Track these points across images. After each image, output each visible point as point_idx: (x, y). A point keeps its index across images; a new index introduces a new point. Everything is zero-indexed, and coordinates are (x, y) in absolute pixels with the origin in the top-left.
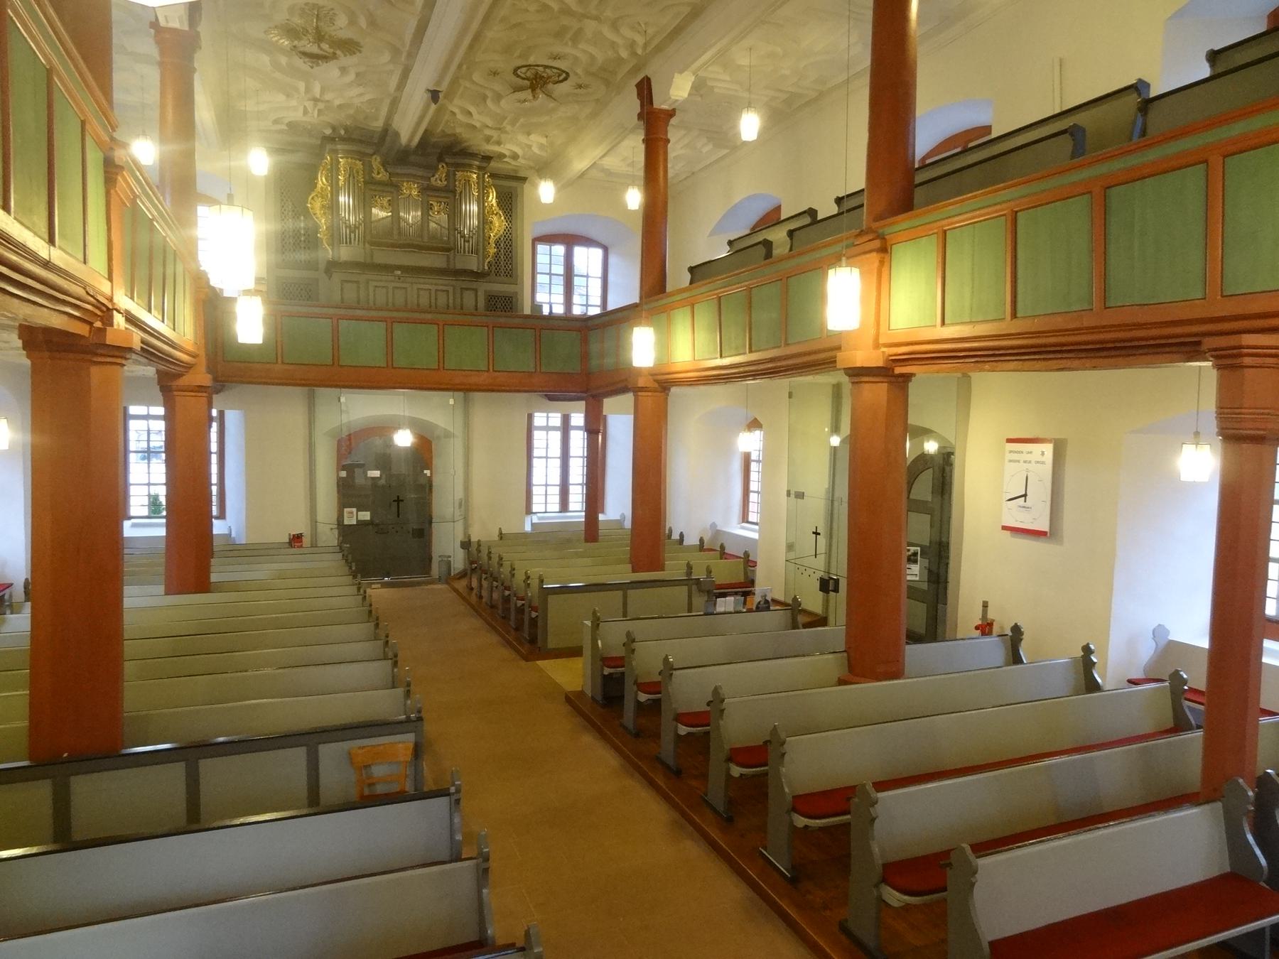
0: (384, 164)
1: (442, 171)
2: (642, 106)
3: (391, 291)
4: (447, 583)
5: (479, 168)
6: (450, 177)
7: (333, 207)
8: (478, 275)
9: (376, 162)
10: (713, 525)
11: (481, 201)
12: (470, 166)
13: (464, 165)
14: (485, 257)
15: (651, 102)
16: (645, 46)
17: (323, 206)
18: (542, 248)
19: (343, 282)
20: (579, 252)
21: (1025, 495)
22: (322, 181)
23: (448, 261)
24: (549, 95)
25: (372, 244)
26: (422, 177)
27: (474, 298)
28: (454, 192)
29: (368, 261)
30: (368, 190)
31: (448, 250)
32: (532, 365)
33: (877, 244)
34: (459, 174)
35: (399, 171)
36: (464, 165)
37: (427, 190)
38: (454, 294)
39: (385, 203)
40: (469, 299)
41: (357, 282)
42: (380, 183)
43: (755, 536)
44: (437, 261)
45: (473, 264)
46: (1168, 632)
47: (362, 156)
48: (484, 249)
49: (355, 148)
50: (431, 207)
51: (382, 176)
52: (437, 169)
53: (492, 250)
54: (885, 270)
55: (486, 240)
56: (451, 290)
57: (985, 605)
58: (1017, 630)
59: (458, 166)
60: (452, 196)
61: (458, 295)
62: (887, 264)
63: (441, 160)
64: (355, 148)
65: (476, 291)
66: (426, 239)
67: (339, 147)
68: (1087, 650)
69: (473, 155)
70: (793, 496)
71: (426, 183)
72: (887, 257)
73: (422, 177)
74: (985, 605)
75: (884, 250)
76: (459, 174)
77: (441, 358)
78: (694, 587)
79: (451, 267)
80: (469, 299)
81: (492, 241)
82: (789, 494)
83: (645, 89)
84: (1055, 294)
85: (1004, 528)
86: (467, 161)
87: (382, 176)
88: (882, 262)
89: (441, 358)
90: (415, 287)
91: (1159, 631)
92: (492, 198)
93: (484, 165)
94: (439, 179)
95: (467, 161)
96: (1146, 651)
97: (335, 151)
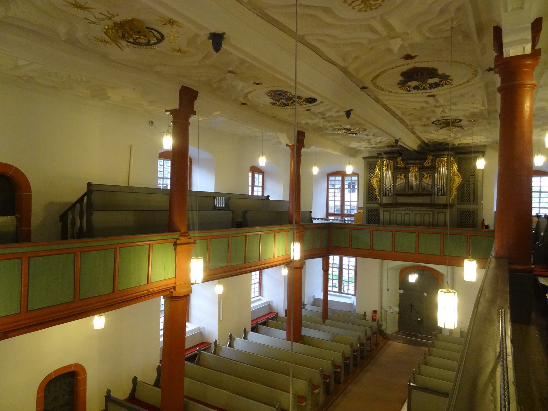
0: (402, 160)
1: (430, 158)
5: (448, 155)
6: (433, 161)
7: (381, 181)
9: (399, 160)
12: (444, 155)
13: (441, 155)
14: (450, 197)
16: (483, 105)
19: (384, 211)
22: (377, 170)
23: (431, 201)
25: (396, 195)
30: (396, 170)
31: (431, 195)
34: (437, 159)
35: (409, 162)
36: (441, 155)
37: (422, 170)
38: (433, 215)
39: (402, 176)
40: (441, 217)
41: (390, 211)
45: (442, 200)
49: (390, 156)
51: (401, 165)
52: (426, 159)
53: (454, 192)
55: (451, 189)
56: (431, 213)
60: (433, 169)
63: (427, 155)
64: (390, 156)
65: (445, 213)
71: (421, 165)
76: (437, 159)
80: (441, 217)
86: (442, 153)
90: (414, 212)
92: (455, 166)
97: (383, 158)
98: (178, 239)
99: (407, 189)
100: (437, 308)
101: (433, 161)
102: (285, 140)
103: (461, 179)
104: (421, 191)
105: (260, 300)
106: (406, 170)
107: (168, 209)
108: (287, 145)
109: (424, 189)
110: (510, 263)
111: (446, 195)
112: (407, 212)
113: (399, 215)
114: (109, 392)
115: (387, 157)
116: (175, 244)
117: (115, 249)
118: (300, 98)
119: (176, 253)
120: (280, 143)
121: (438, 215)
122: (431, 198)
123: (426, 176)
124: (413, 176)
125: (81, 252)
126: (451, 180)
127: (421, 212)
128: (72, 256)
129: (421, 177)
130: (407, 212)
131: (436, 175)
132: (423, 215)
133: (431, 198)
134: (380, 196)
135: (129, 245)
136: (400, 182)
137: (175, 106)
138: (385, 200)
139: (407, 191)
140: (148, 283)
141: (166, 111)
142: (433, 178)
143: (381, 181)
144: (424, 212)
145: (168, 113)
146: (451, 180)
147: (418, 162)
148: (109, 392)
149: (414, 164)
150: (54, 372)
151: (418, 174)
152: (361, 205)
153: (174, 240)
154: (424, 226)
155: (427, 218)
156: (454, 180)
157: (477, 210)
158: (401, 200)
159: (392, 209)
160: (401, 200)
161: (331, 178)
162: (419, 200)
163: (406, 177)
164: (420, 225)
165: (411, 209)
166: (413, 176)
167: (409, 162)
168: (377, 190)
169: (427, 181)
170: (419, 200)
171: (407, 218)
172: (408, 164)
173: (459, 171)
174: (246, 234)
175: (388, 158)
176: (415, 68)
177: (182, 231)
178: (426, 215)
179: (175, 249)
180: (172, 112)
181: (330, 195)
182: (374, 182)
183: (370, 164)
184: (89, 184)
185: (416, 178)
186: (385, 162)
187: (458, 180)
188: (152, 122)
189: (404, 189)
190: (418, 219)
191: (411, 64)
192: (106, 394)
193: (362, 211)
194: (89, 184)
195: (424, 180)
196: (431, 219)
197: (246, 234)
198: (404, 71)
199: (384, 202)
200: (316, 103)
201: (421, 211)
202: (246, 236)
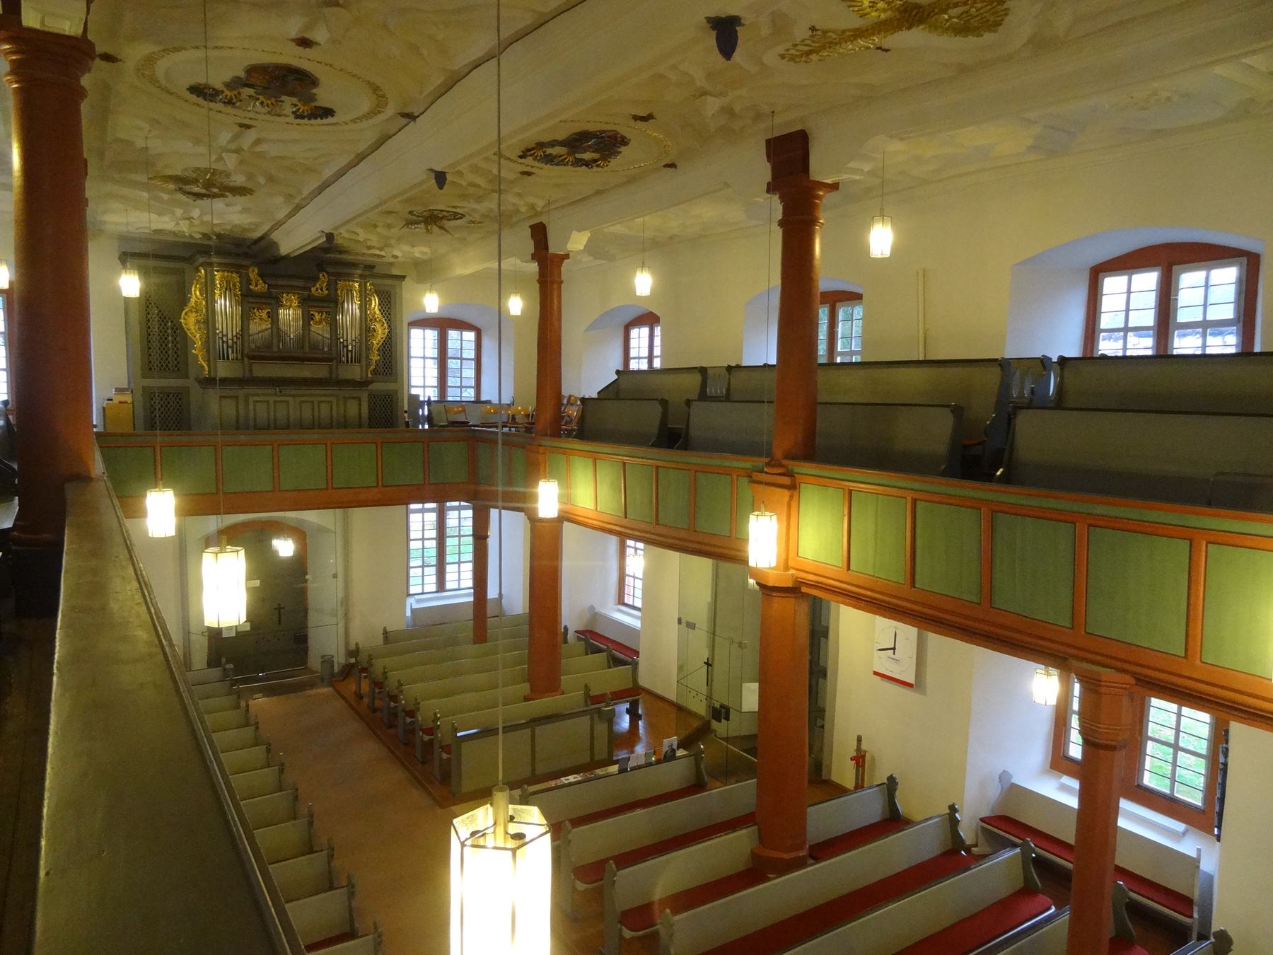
1: (324, 278)
2: (536, 247)
3: (272, 405)
4: (331, 684)
5: (361, 276)
7: (208, 320)
8: (363, 384)
9: (253, 273)
10: (592, 608)
11: (364, 307)
12: (352, 275)
14: (368, 365)
15: (547, 248)
17: (198, 322)
18: (416, 333)
19: (221, 397)
20: (453, 334)
21: (894, 649)
22: (196, 294)
23: (331, 372)
24: (442, 228)
27: (357, 408)
28: (336, 302)
29: (247, 374)
31: (331, 360)
32: (421, 476)
33: (786, 480)
34: (341, 284)
37: (307, 303)
39: (264, 314)
41: (236, 397)
43: (636, 624)
44: (320, 371)
46: (1011, 777)
47: (238, 268)
48: (367, 357)
50: (311, 317)
51: (260, 287)
52: (316, 279)
53: (375, 357)
54: (794, 504)
55: (369, 348)
57: (859, 740)
58: (891, 779)
59: (339, 276)
60: (332, 304)
61: (341, 402)
62: (795, 498)
66: (307, 349)
67: (215, 260)
68: (953, 809)
69: (354, 265)
70: (684, 625)
71: (306, 293)
72: (796, 493)
74: (859, 740)
75: (793, 487)
76: (341, 284)
78: (596, 716)
81: (376, 347)
82: (680, 621)
83: (539, 233)
84: (943, 577)
85: (876, 673)
86: (345, 271)
88: (791, 497)
90: (298, 399)
91: (1004, 776)
93: (367, 273)
94: (319, 288)
95: (345, 271)
96: (994, 792)
101: (332, 286)
104: (305, 352)
106: (271, 301)
109: (314, 347)
112: (278, 399)
113: (261, 405)
115: (219, 264)
123: (317, 317)
124: (290, 315)
129: (308, 318)
130: (278, 399)
131: (339, 317)
134: (209, 361)
136: (259, 326)
138: (223, 370)
142: (334, 325)
147: (301, 283)
149: (290, 289)
151: (299, 312)
154: (320, 428)
155: (325, 411)
157: (396, 392)
158: (261, 370)
159: (241, 393)
160: (261, 370)
162: (305, 372)
163: (273, 316)
164: (268, 427)
166: (290, 315)
167: (280, 282)
169: (320, 330)
170: (305, 372)
172: (277, 287)
175: (224, 267)
178: (325, 405)
182: (190, 322)
185: (295, 320)
186: (218, 275)
187: (381, 332)
189: (269, 346)
190: (307, 414)
193: (128, 398)
195: (314, 328)
201: (310, 395)
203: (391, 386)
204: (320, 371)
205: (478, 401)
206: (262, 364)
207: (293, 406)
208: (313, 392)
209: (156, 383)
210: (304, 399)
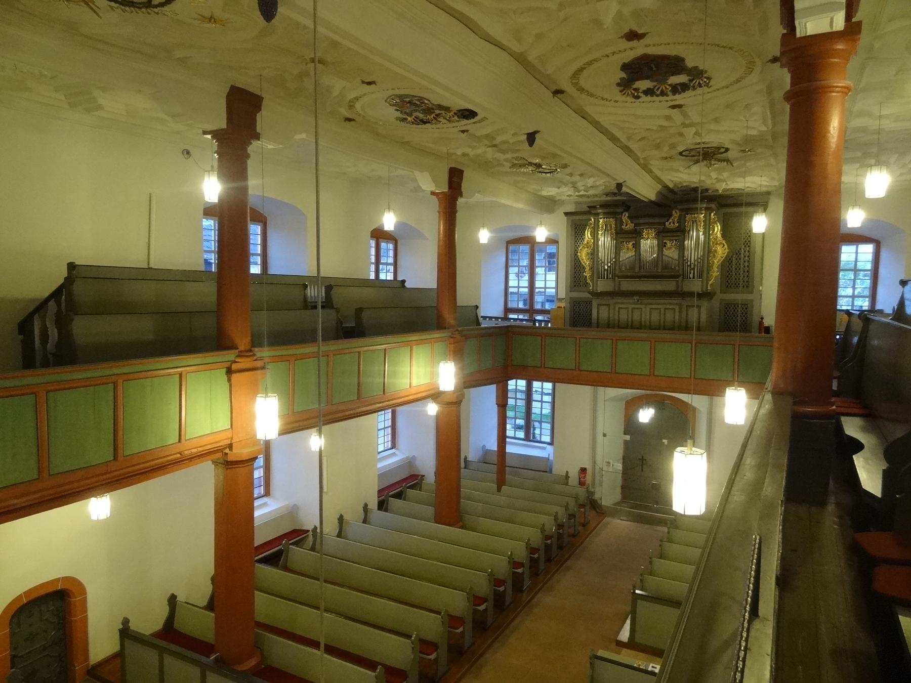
1: (676, 214)
5: (706, 209)
6: (681, 220)
7: (594, 254)
9: (625, 217)
14: (708, 280)
16: (765, 123)
22: (588, 235)
26: (660, 224)
27: (699, 313)
30: (620, 235)
34: (688, 217)
36: (693, 209)
37: (663, 234)
38: (680, 312)
39: (630, 245)
41: (608, 305)
42: (627, 232)
44: (670, 286)
45: (696, 286)
47: (613, 214)
49: (612, 210)
51: (630, 226)
52: (671, 216)
53: (715, 273)
55: (710, 267)
56: (677, 308)
60: (681, 233)
63: (671, 209)
67: (600, 211)
71: (662, 227)
73: (660, 224)
77: (652, 366)
79: (680, 290)
80: (693, 315)
87: (630, 226)
89: (652, 366)
90: (649, 307)
92: (718, 228)
97: (598, 214)
98: (235, 362)
99: (637, 270)
100: (671, 480)
101: (681, 220)
102: (429, 183)
103: (727, 250)
104: (662, 271)
105: (394, 454)
106: (636, 235)
107: (214, 308)
108: (433, 193)
109: (666, 267)
110: (795, 403)
111: (700, 276)
113: (624, 311)
114: (126, 622)
115: (604, 213)
116: (229, 372)
117: (115, 384)
118: (447, 109)
119: (231, 386)
120: (418, 189)
121: (687, 311)
122: (677, 282)
123: (669, 245)
124: (648, 244)
125: (48, 392)
126: (709, 252)
127: (659, 307)
128: (30, 399)
129: (662, 246)
131: (686, 242)
132: (662, 311)
133: (677, 282)
134: (592, 280)
135: (131, 376)
136: (627, 255)
137: (221, 123)
138: (602, 286)
139: (639, 271)
140: (180, 441)
141: (205, 133)
142: (682, 248)
143: (594, 254)
144: (665, 306)
145: (209, 137)
146: (709, 252)
147: (657, 220)
148: (126, 622)
149: (650, 225)
150: (27, 593)
151: (655, 242)
152: (562, 294)
153: (227, 364)
154: (665, 329)
155: (669, 317)
156: (716, 251)
157: (752, 301)
158: (627, 285)
159: (611, 302)
161: (511, 247)
163: (637, 246)
165: (645, 301)
166: (648, 244)
167: (642, 221)
168: (587, 269)
169: (671, 253)
171: (636, 318)
172: (639, 224)
173: (723, 236)
174: (357, 350)
175: (607, 215)
176: (645, 57)
177: (242, 348)
179: (229, 380)
180: (216, 134)
181: (512, 276)
182: (584, 255)
183: (578, 222)
184: (71, 266)
185: (652, 247)
186: (601, 221)
187: (721, 251)
188: (188, 153)
189: (632, 267)
190: (655, 317)
191: (638, 49)
192: (121, 627)
193: (563, 305)
194: (71, 266)
195: (666, 252)
196: (677, 318)
197: (357, 350)
198: (627, 61)
199: (600, 289)
200: (476, 119)
201: (659, 304)
202: (359, 352)
203: (739, 297)
204: (670, 286)
205: (872, 309)
206: (631, 281)
207: (648, 312)
208: (662, 301)
209: (575, 295)
210: (653, 307)
